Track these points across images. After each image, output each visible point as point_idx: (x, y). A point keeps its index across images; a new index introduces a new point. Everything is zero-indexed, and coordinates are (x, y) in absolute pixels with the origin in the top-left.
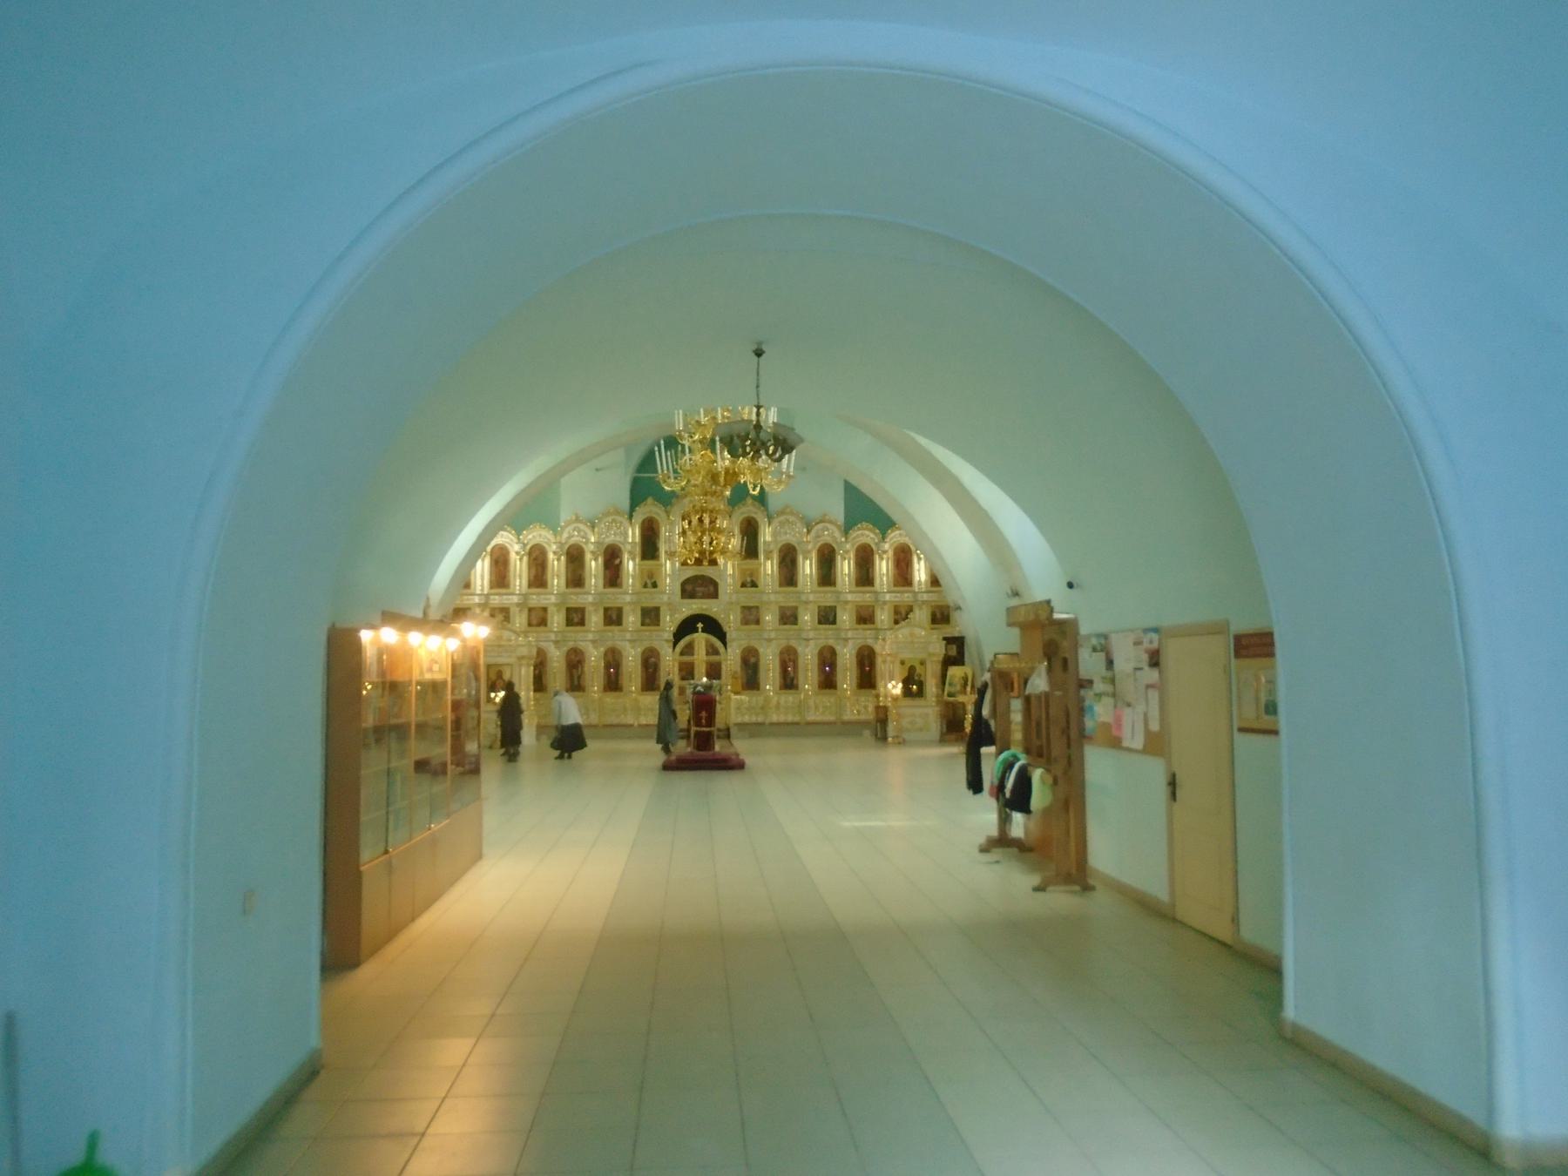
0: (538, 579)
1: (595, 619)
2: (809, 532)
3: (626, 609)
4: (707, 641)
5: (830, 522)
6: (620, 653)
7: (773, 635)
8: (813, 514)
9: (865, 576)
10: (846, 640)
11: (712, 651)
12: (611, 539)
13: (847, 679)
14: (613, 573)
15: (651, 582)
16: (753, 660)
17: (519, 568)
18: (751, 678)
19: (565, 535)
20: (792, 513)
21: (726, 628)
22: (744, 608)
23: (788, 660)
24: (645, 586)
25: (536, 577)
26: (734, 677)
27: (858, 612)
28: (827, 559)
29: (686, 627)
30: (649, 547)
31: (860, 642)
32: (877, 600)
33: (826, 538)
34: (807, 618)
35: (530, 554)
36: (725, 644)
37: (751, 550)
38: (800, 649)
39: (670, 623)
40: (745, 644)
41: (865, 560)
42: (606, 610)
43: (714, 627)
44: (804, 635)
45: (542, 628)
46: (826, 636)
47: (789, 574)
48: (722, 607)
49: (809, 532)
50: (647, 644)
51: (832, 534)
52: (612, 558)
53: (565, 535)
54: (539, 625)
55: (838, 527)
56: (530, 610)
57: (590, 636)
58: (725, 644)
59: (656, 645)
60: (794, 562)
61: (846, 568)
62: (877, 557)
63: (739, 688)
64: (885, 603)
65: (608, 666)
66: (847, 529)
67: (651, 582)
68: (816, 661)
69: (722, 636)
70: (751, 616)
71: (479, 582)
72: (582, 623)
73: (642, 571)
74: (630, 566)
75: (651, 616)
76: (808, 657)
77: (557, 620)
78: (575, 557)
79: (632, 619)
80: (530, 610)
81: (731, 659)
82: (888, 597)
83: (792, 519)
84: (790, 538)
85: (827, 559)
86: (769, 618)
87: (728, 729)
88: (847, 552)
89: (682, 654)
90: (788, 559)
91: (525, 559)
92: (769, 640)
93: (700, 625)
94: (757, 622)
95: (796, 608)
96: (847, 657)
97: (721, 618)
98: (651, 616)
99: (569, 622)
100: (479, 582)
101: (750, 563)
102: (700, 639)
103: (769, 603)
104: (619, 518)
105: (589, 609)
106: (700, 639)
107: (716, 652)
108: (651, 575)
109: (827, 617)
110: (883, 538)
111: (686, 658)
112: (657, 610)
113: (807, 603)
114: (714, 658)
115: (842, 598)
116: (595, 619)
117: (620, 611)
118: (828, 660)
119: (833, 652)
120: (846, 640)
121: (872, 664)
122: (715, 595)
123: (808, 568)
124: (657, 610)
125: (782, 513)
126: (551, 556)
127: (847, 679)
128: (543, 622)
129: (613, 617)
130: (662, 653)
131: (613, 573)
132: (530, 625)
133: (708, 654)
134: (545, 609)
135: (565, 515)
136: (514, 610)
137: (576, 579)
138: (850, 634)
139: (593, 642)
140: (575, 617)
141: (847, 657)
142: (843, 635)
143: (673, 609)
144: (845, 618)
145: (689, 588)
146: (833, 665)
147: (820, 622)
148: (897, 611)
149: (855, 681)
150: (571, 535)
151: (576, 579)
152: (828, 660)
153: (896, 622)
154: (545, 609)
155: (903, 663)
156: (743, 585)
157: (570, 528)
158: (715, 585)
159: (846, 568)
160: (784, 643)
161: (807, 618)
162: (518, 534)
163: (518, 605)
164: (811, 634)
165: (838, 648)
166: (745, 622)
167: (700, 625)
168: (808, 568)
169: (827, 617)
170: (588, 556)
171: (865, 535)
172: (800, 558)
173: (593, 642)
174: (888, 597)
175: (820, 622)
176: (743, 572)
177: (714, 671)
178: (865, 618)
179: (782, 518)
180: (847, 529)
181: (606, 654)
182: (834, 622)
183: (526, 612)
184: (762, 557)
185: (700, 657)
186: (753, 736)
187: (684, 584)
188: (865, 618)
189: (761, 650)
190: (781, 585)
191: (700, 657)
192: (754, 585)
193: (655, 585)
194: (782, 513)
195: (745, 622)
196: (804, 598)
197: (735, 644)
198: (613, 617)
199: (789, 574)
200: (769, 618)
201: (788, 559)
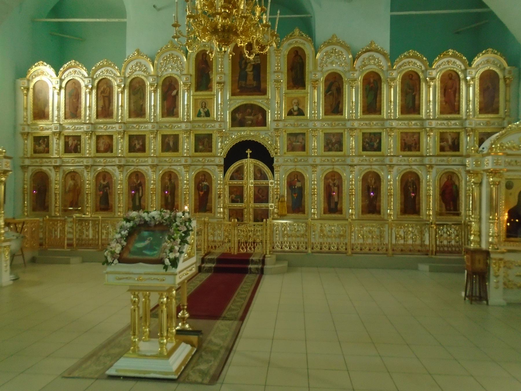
0: (105, 110)
1: (154, 145)
2: (354, 59)
3: (182, 137)
4: (255, 166)
5: (377, 51)
6: (176, 177)
7: (318, 161)
8: (359, 44)
9: (411, 105)
10: (391, 166)
11: (260, 175)
12: (170, 72)
13: (391, 204)
14: (170, 105)
15: (204, 111)
16: (298, 184)
17: (89, 101)
18: (296, 204)
19: (129, 71)
20: (338, 43)
21: (272, 154)
22: (290, 135)
23: (333, 186)
24: (199, 115)
25: (104, 107)
26: (280, 200)
27: (403, 139)
28: (373, 86)
29: (236, 153)
30: (203, 78)
31: (405, 169)
32: (423, 128)
33: (372, 67)
34: (352, 143)
35: (98, 88)
36: (272, 169)
37: (297, 76)
38: (344, 175)
39: (221, 147)
40: (291, 168)
41: (411, 86)
42: (164, 137)
43: (261, 153)
44: (349, 161)
45: (108, 154)
46: (370, 162)
47: (334, 104)
48: (271, 135)
49: (354, 59)
50: (199, 168)
51: (379, 63)
52: (169, 90)
53: (129, 71)
54: (106, 151)
55: (384, 55)
56: (98, 137)
57: (150, 161)
58: (272, 169)
59: (209, 169)
60: (340, 91)
61: (391, 96)
62: (424, 86)
63: (285, 212)
64: (431, 129)
65: (164, 188)
66: (393, 57)
67: (204, 111)
68: (360, 184)
69: (269, 161)
70: (297, 142)
71: (56, 113)
72: (143, 149)
73: (195, 100)
74: (186, 99)
75: (204, 143)
76: (352, 182)
77: (121, 145)
78: (136, 89)
79: (187, 145)
80: (98, 137)
81: (277, 183)
82: (434, 124)
83: (338, 48)
84: (335, 67)
85: (373, 86)
86: (316, 144)
87: (263, 262)
88: (393, 79)
89: (232, 178)
90: (334, 87)
91: (94, 92)
92: (314, 166)
93: (249, 152)
94: (303, 148)
95: (341, 135)
96: (391, 182)
97: (267, 144)
98: (204, 143)
99: (132, 149)
100: (56, 113)
101: (297, 93)
102: (249, 164)
103: (315, 130)
104: (176, 53)
105: (150, 137)
106: (249, 164)
107: (264, 177)
108: (204, 105)
109: (372, 143)
110: (431, 65)
111: (235, 182)
112: (210, 136)
113: (352, 129)
114: (263, 182)
115: (387, 124)
116: (154, 145)
117: (176, 137)
118: (372, 186)
119: (378, 178)
120: (391, 166)
121: (417, 190)
122: (263, 123)
123: (353, 98)
124: (210, 136)
125: (328, 43)
126: (116, 90)
127: (391, 204)
128: (109, 148)
129: (170, 144)
130: (214, 177)
131: (170, 105)
132: (98, 151)
133: (255, 179)
134: (111, 137)
135: (130, 52)
136: (85, 138)
137: (138, 110)
138: (395, 160)
139: (153, 166)
140: (137, 144)
141: (391, 182)
142: (387, 161)
143: (224, 136)
144: (390, 144)
145: (239, 116)
146: (377, 190)
147: (364, 149)
148: (443, 137)
149: (398, 206)
150: (132, 71)
151: (138, 110)
152: (372, 186)
153: (442, 149)
154: (111, 137)
155: (509, 186)
156: (290, 113)
157: (133, 63)
158: (264, 113)
159: (391, 96)
160: (328, 169)
161: (352, 143)
162: (88, 70)
163: (86, 133)
164: (356, 160)
165: (382, 174)
166: (291, 148)
167: (249, 152)
168: (353, 98)
169: (372, 143)
170: (148, 89)
171: (413, 63)
172: (346, 87)
173: (153, 166)
174: (434, 124)
175: (364, 149)
176: (290, 101)
177: (262, 195)
178: (410, 144)
179: (329, 48)
180: (393, 57)
181: (163, 178)
182: (379, 149)
183: (94, 138)
184: (309, 87)
185: (249, 183)
186: (291, 267)
187: (234, 113)
188: (410, 144)
189: (307, 176)
190: (326, 113)
191: (249, 183)
192: (301, 113)
193: (208, 114)
194: (328, 43)
195: (291, 148)
196: (349, 125)
197: (281, 169)
198: (170, 144)
199: (334, 104)
200: (316, 144)
201: (334, 87)
